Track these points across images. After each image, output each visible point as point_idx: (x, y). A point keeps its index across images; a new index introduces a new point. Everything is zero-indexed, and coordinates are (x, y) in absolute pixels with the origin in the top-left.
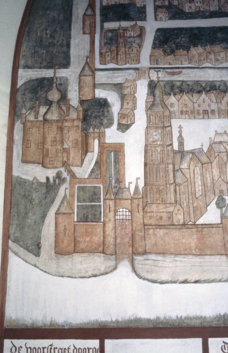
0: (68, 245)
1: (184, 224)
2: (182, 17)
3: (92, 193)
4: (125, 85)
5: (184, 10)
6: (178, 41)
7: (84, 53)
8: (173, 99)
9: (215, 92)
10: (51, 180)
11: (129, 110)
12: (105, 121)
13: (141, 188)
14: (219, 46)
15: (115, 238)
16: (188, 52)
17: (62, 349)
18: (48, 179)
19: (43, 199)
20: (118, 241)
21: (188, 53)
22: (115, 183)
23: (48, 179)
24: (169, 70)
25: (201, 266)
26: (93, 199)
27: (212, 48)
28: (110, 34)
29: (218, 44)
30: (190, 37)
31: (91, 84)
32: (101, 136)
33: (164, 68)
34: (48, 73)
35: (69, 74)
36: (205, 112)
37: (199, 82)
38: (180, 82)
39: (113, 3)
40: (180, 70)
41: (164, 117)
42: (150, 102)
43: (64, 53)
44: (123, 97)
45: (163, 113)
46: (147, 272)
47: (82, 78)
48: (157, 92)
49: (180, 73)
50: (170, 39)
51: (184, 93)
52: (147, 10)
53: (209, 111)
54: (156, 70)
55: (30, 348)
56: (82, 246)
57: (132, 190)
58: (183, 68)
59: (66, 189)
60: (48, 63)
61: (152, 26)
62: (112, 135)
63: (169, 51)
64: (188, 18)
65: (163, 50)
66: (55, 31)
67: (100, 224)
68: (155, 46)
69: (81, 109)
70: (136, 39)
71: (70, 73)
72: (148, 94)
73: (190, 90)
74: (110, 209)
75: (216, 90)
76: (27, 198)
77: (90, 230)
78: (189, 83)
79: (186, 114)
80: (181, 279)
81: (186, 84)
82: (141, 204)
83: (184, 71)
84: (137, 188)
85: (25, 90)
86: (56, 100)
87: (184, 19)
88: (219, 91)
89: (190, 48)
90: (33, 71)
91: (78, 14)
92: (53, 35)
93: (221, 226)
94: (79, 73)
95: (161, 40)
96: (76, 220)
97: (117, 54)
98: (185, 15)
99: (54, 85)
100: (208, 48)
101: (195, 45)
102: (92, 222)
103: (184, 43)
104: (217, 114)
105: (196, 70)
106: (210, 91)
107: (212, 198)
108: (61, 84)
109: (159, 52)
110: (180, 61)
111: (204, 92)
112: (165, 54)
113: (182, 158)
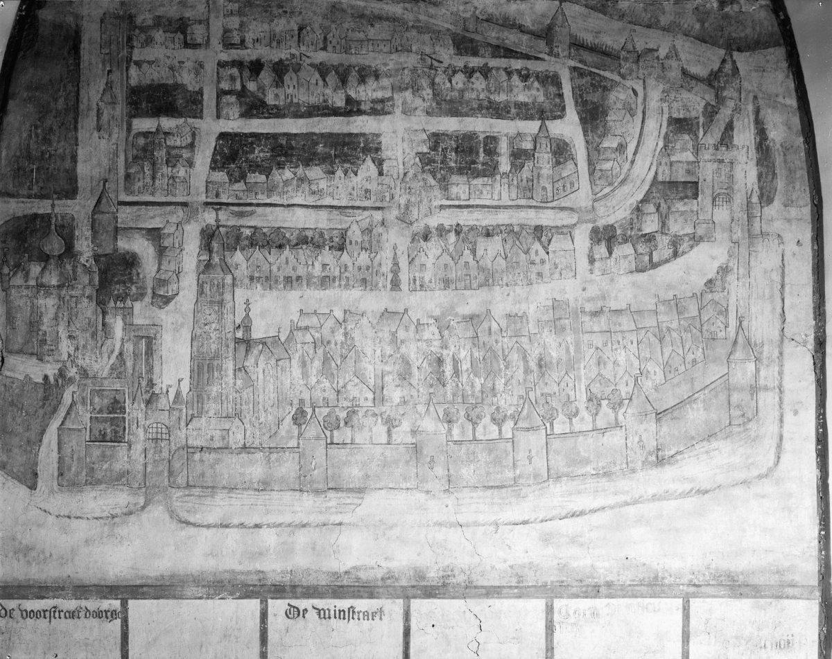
0: (78, 474)
1: (244, 447)
2: (263, 113)
3: (112, 401)
4: (166, 231)
5: (266, 100)
7: (100, 173)
8: (239, 257)
9: (304, 247)
10: (52, 379)
11: (170, 273)
12: (134, 288)
13: (184, 394)
14: (318, 168)
15: (145, 465)
16: (267, 177)
17: (69, 612)
18: (46, 377)
19: (40, 407)
20: (149, 469)
22: (148, 385)
23: (46, 377)
24: (236, 209)
25: (265, 506)
26: (113, 409)
27: (307, 172)
28: (141, 141)
29: (316, 165)
30: (272, 150)
31: (111, 228)
32: (128, 313)
33: (228, 204)
34: (43, 207)
35: (78, 209)
36: (288, 280)
37: (282, 230)
38: (253, 230)
39: (149, 82)
40: (253, 208)
41: (223, 287)
42: (204, 261)
43: (67, 171)
44: (161, 252)
45: (223, 280)
46: (188, 512)
47: (96, 217)
48: (215, 245)
49: (252, 213)
50: (240, 152)
52: (205, 97)
53: (294, 278)
54: (216, 207)
55: (26, 611)
56: (99, 475)
57: (172, 396)
58: (258, 205)
59: (74, 392)
60: (42, 188)
61: (211, 128)
62: (142, 312)
63: (237, 174)
65: (228, 173)
66: (51, 129)
67: (123, 444)
68: (215, 166)
69: (95, 269)
70: (184, 151)
71: (77, 208)
72: (201, 248)
73: (266, 244)
74: (137, 423)
76: (16, 406)
77: (108, 453)
78: (265, 230)
79: (258, 282)
80: (236, 521)
82: (184, 417)
83: (260, 210)
84: (178, 394)
85: (6, 234)
86: (56, 253)
87: (265, 118)
90: (18, 202)
91: (89, 100)
92: (48, 137)
93: (297, 450)
94: (92, 208)
96: (88, 439)
97: (154, 178)
99: (53, 227)
100: (300, 171)
101: (280, 166)
102: (112, 442)
104: (304, 283)
105: (277, 209)
106: (297, 244)
107: (287, 411)
108: (63, 226)
109: (220, 176)
111: (288, 247)
112: (230, 180)
113: (247, 351)
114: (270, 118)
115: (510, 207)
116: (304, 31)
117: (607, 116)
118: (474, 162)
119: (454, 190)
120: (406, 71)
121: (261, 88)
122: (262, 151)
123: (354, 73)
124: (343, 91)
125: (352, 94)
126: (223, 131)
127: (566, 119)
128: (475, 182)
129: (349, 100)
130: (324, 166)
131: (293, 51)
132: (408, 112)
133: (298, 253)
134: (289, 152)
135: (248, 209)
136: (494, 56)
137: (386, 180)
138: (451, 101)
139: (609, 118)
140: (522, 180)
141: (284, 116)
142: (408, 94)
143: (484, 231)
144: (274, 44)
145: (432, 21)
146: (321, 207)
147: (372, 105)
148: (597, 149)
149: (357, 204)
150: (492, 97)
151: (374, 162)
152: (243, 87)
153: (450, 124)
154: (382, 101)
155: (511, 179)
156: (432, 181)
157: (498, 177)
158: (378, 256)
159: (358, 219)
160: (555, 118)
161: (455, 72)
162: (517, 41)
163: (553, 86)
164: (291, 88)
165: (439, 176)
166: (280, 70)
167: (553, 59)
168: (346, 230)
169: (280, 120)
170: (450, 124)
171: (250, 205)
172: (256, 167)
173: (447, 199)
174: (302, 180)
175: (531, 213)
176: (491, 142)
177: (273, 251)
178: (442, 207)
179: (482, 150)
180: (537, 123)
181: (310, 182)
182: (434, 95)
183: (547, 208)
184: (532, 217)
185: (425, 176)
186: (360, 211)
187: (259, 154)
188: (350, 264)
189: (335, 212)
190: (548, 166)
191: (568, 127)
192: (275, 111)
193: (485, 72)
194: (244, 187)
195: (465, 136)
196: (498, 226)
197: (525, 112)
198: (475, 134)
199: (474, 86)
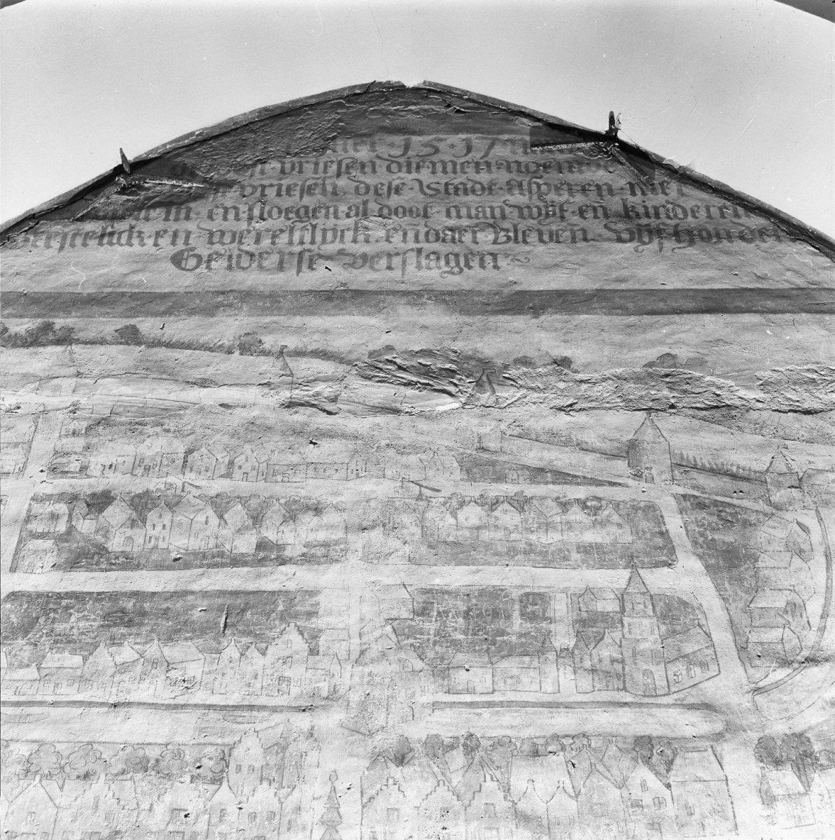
6: (59, 627)
9: (139, 776)
14: (189, 643)
16: (85, 659)
21: (84, 663)
29: (186, 639)
30: (104, 618)
38: (35, 746)
49: (38, 720)
50: (42, 620)
51: (38, 778)
64: (113, 567)
75: (146, 771)
78: (59, 747)
81: (52, 749)
87: (102, 570)
88: (153, 773)
89: (96, 647)
95: (13, 623)
98: (108, 559)
100: (153, 650)
101: (114, 641)
103: (83, 633)
110: (52, 685)
114: (110, 570)
115: (581, 704)
116: (195, 454)
117: (756, 561)
118: (503, 633)
119: (461, 677)
120: (373, 504)
121: (106, 531)
122: (85, 618)
123: (277, 507)
124: (254, 531)
125: (271, 535)
126: (17, 589)
127: (679, 565)
128: (504, 664)
129: (261, 546)
130: (201, 641)
131: (171, 479)
132: (373, 557)
133: (122, 789)
134: (137, 620)
135: (36, 710)
136: (533, 480)
137: (324, 663)
138: (455, 544)
139: (760, 564)
140: (600, 661)
141: (138, 567)
142: (376, 535)
143: (526, 747)
144: (139, 471)
145: (421, 438)
146: (184, 706)
147: (305, 550)
148: (747, 610)
149: (262, 701)
150: (533, 537)
151: (301, 634)
152: (71, 530)
153: (455, 577)
154: (326, 545)
155: (577, 660)
156: (419, 665)
157: (551, 656)
158: (296, 794)
159: (259, 727)
160: (657, 565)
161: (462, 504)
162: (574, 462)
163: (648, 521)
164: (159, 528)
165: (430, 654)
166: (142, 505)
167: (643, 484)
168: (232, 747)
169: (128, 573)
170: (455, 577)
171: (41, 703)
172: (64, 641)
173: (448, 692)
174: (155, 663)
175: (625, 715)
176: (534, 604)
177: (69, 785)
178: (435, 706)
179: (516, 614)
180: (626, 574)
181: (169, 666)
182: (423, 534)
183: (659, 706)
184: (628, 722)
185: (403, 655)
186: (266, 714)
187: (76, 623)
188: (232, 809)
189: (213, 715)
190: (651, 638)
191: (687, 577)
192: (121, 559)
193: (521, 503)
194: (36, 675)
195: (482, 593)
196: (556, 737)
197: (596, 555)
198: (502, 590)
199: (499, 523)
